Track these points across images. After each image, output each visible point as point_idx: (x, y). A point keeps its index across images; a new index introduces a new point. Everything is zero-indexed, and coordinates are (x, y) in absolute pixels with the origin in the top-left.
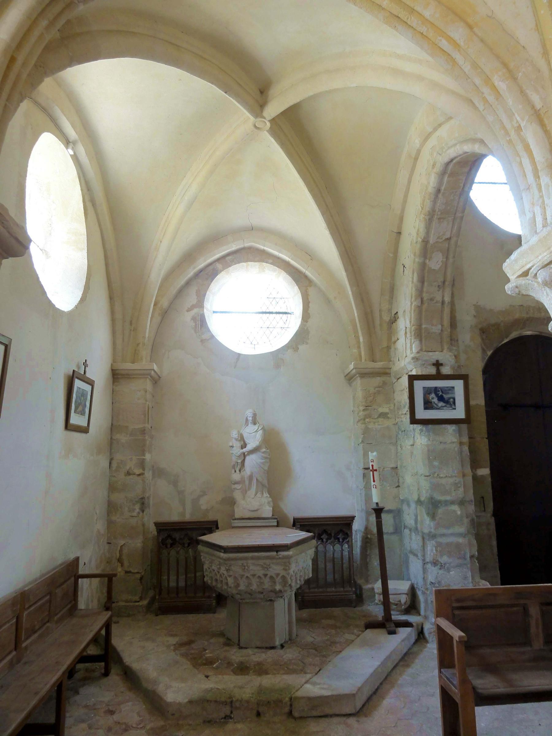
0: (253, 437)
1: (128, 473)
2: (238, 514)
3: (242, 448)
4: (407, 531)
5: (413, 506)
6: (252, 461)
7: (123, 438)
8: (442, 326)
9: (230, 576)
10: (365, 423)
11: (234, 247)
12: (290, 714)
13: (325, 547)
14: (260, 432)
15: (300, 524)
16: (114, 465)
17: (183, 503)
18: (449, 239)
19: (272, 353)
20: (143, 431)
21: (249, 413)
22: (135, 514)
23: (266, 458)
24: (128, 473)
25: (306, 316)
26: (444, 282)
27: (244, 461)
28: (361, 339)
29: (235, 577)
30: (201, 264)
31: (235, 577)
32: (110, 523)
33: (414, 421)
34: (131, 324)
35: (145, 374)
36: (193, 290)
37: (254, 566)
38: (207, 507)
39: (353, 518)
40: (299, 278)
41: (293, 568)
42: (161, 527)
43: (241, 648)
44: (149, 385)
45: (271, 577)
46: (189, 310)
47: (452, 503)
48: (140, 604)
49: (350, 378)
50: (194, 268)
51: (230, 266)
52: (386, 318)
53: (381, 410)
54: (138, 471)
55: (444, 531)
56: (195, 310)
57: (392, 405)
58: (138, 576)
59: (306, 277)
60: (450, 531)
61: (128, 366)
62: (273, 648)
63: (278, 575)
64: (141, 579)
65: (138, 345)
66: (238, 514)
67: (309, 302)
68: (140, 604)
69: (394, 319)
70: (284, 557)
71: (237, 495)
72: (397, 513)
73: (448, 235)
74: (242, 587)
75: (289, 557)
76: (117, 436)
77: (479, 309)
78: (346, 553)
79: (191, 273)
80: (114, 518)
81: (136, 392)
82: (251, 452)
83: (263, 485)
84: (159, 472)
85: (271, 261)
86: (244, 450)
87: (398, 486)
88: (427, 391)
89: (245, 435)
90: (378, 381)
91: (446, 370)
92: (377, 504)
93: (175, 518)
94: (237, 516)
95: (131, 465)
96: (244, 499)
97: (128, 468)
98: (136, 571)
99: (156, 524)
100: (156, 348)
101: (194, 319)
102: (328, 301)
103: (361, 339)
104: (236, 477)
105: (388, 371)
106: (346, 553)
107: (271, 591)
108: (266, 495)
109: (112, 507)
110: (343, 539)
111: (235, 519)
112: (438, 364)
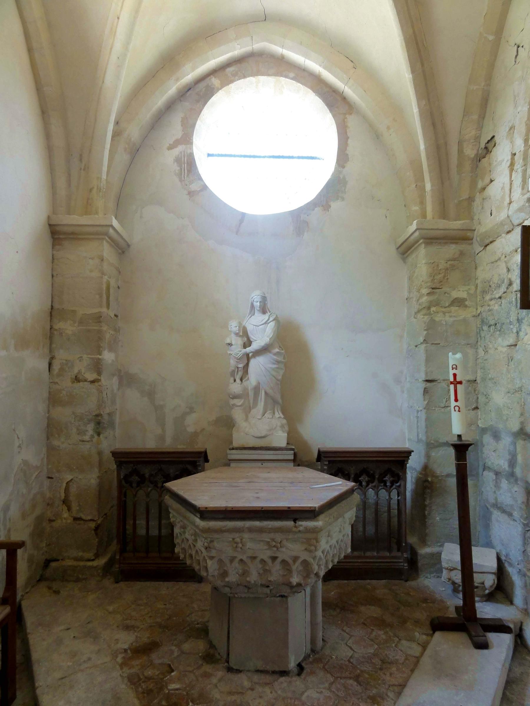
0: (262, 331)
1: (77, 379)
2: (238, 439)
3: (245, 347)
4: (489, 476)
5: (506, 440)
6: (258, 366)
7: (68, 327)
9: (212, 558)
10: (430, 314)
11: (236, 50)
13: (365, 494)
14: (272, 324)
16: (56, 367)
19: (292, 213)
20: (98, 318)
21: (256, 297)
22: (87, 438)
23: (278, 362)
24: (77, 379)
27: (247, 365)
28: (428, 186)
29: (220, 561)
31: (220, 561)
32: (51, 449)
34: (81, 160)
35: (101, 233)
37: (254, 543)
38: (191, 428)
39: (408, 453)
40: (334, 100)
41: (324, 544)
43: (230, 670)
45: (284, 562)
46: (171, 148)
48: (95, 563)
50: (178, 80)
51: (232, 82)
52: (470, 152)
53: (455, 294)
54: (91, 376)
56: (180, 148)
57: (473, 287)
58: (93, 525)
59: (344, 99)
61: (76, 219)
62: (284, 673)
63: (295, 559)
64: (96, 529)
65: (91, 190)
67: (348, 138)
68: (95, 563)
69: (489, 146)
70: (308, 530)
71: (238, 415)
74: (232, 578)
75: (315, 531)
76: (59, 325)
78: (394, 502)
79: (172, 89)
80: (56, 443)
81: (88, 261)
82: (258, 353)
83: (275, 402)
84: (126, 379)
85: (292, 75)
86: (248, 350)
87: (477, 408)
89: (250, 328)
90: (452, 250)
92: (459, 436)
93: (150, 444)
94: (235, 444)
95: (82, 367)
96: (247, 419)
97: (76, 371)
98: (89, 518)
99: (115, 454)
101: (178, 160)
103: (428, 186)
104: (236, 387)
105: (469, 234)
106: (394, 502)
107: (283, 584)
108: (278, 414)
109: (52, 428)
110: (392, 483)
111: (233, 449)
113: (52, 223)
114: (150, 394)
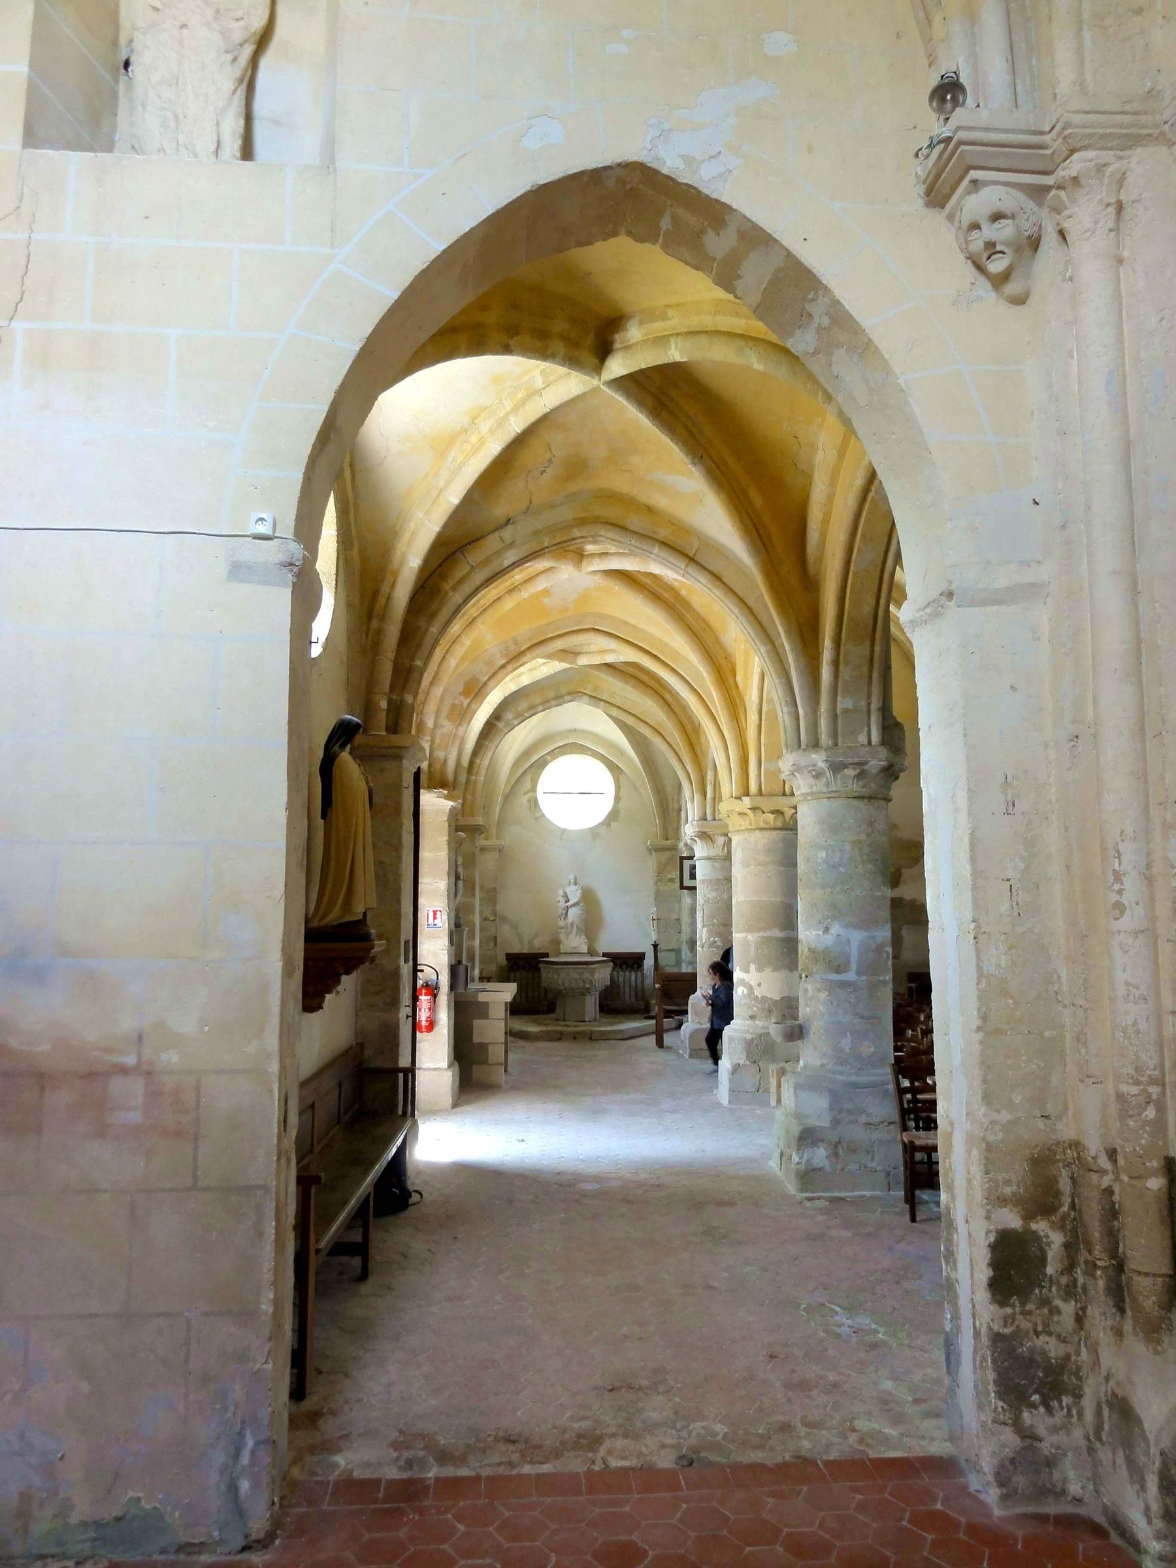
0: (575, 895)
6: (573, 914)
12: (591, 1038)
15: (604, 955)
17: (521, 942)
20: (495, 890)
25: (617, 798)
30: (535, 758)
33: (682, 887)
36: (528, 778)
37: (574, 974)
38: (539, 945)
39: (644, 954)
40: (612, 767)
41: (597, 976)
42: (510, 957)
44: (496, 855)
49: (650, 851)
52: (676, 807)
53: (670, 876)
54: (492, 918)
66: (563, 949)
71: (562, 937)
72: (678, 952)
79: (527, 765)
82: (572, 906)
84: (504, 920)
90: (667, 854)
100: (500, 824)
102: (635, 787)
104: (561, 923)
106: (639, 981)
108: (583, 937)
114: (515, 927)
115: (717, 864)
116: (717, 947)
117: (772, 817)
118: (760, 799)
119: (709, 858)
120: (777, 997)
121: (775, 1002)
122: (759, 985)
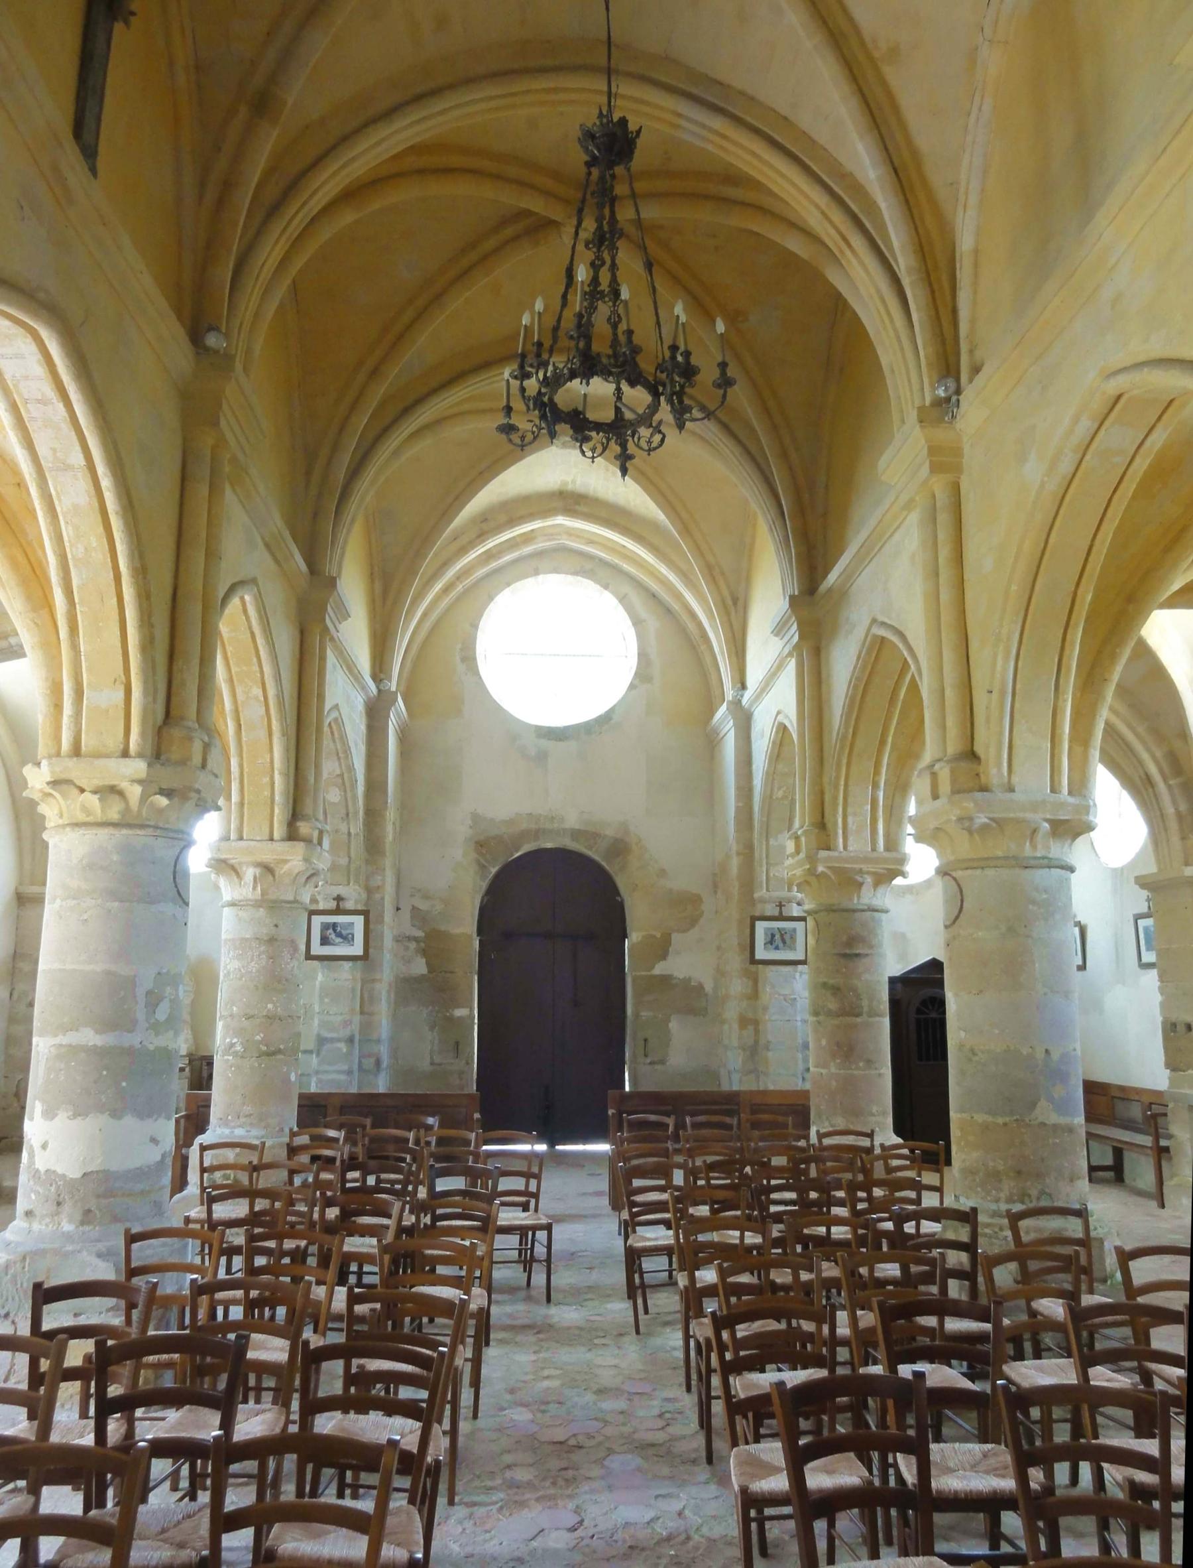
8: (349, 857)
16: (15, 996)
18: (342, 776)
26: (347, 815)
33: (309, 957)
47: (339, 1040)
55: (327, 1068)
60: (335, 1068)
73: (338, 772)
77: (476, 818)
88: (325, 927)
91: (350, 905)
112: (339, 899)
113: (21, 890)
115: (242, 914)
116: (235, 1054)
117: (93, 800)
118: (71, 763)
119: (232, 904)
120: (75, 1174)
121: (72, 1185)
122: (44, 1146)
